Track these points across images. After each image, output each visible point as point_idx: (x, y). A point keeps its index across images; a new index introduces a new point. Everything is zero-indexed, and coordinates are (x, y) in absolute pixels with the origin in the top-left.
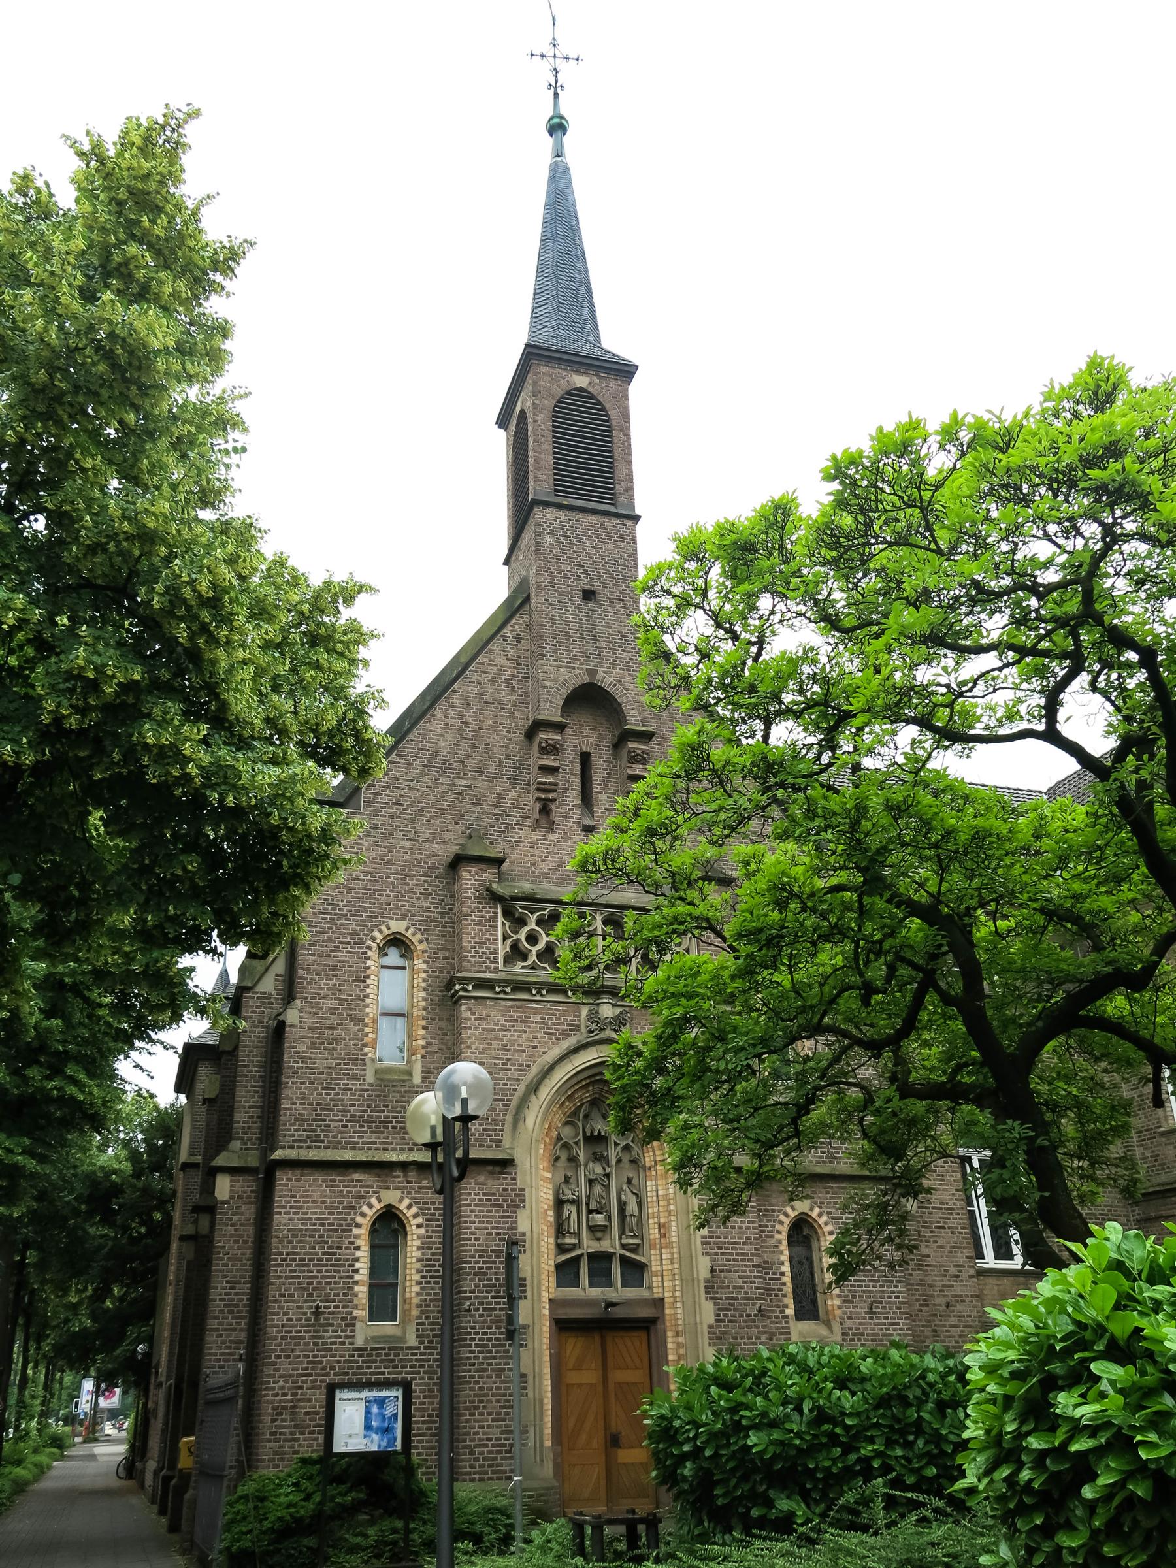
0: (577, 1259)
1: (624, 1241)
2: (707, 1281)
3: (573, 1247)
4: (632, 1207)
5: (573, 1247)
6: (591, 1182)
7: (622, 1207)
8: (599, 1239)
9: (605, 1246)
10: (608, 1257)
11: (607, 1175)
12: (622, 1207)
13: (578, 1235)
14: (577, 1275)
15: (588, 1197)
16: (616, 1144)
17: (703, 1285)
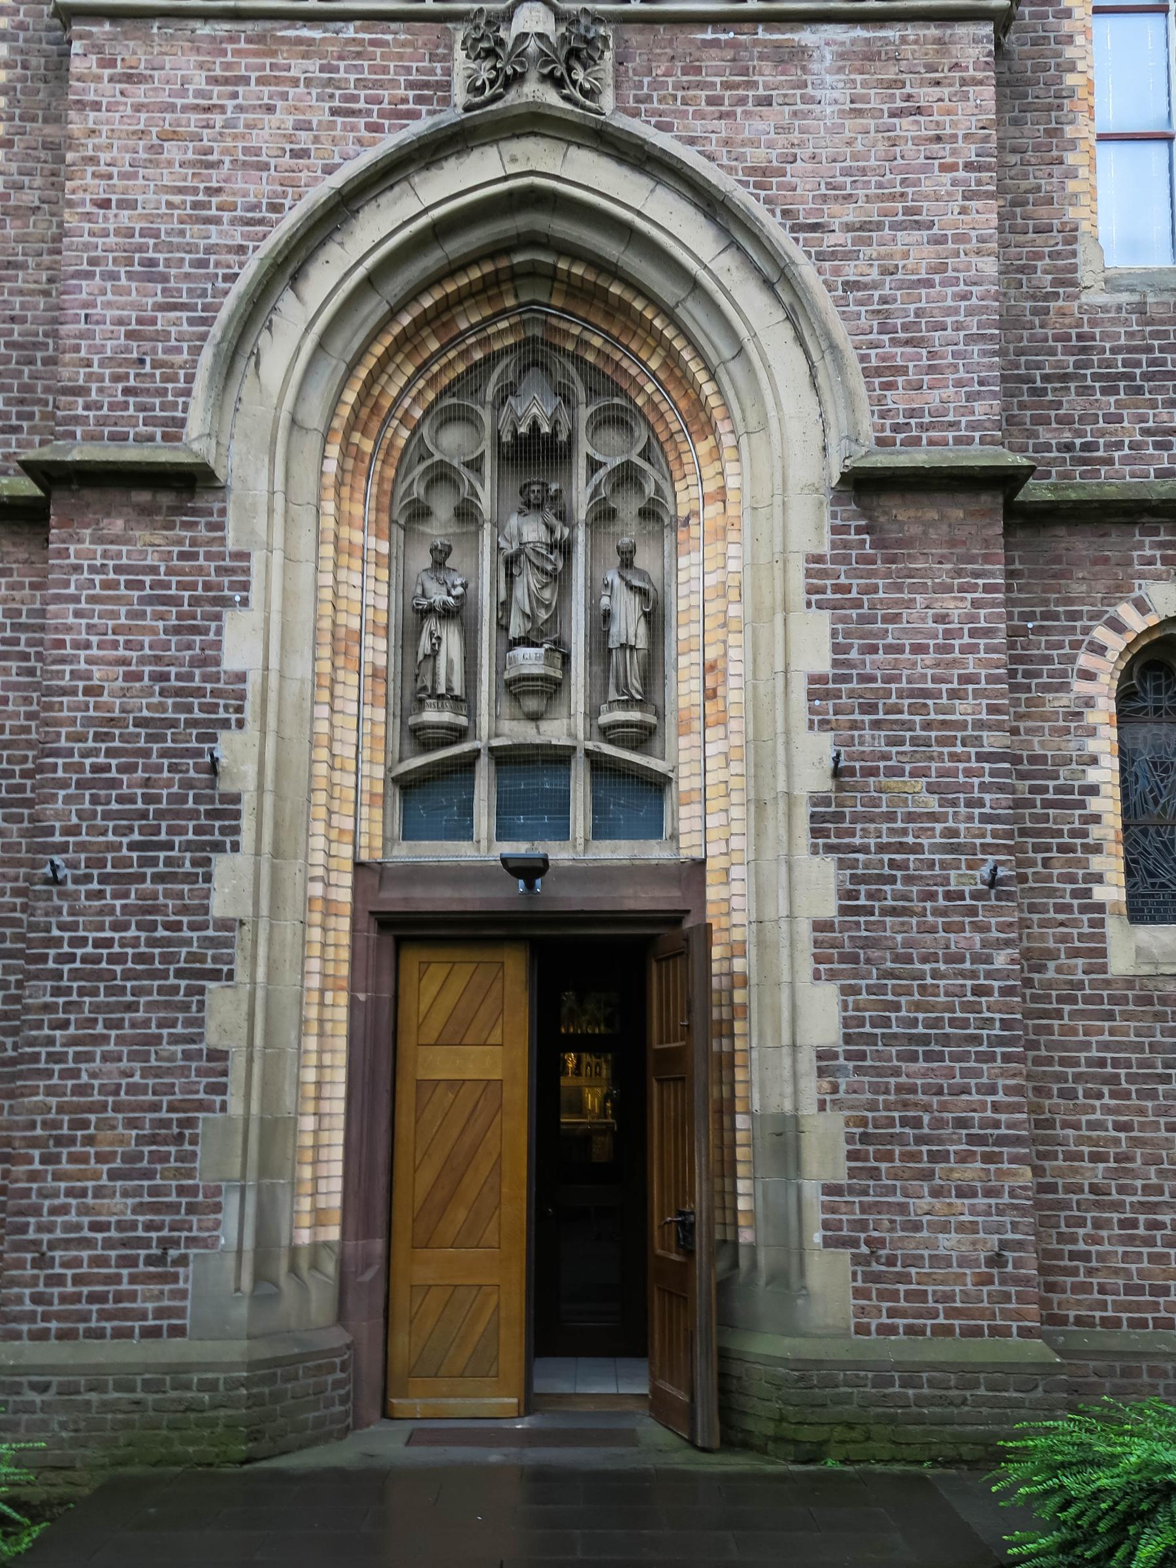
0: (467, 764)
1: (605, 719)
2: (818, 800)
3: (459, 734)
4: (628, 623)
5: (459, 734)
6: (511, 562)
7: (602, 620)
8: (534, 718)
9: (554, 732)
10: (558, 758)
11: (565, 549)
12: (602, 620)
13: (465, 702)
14: (467, 810)
15: (504, 607)
16: (594, 466)
17: (803, 813)
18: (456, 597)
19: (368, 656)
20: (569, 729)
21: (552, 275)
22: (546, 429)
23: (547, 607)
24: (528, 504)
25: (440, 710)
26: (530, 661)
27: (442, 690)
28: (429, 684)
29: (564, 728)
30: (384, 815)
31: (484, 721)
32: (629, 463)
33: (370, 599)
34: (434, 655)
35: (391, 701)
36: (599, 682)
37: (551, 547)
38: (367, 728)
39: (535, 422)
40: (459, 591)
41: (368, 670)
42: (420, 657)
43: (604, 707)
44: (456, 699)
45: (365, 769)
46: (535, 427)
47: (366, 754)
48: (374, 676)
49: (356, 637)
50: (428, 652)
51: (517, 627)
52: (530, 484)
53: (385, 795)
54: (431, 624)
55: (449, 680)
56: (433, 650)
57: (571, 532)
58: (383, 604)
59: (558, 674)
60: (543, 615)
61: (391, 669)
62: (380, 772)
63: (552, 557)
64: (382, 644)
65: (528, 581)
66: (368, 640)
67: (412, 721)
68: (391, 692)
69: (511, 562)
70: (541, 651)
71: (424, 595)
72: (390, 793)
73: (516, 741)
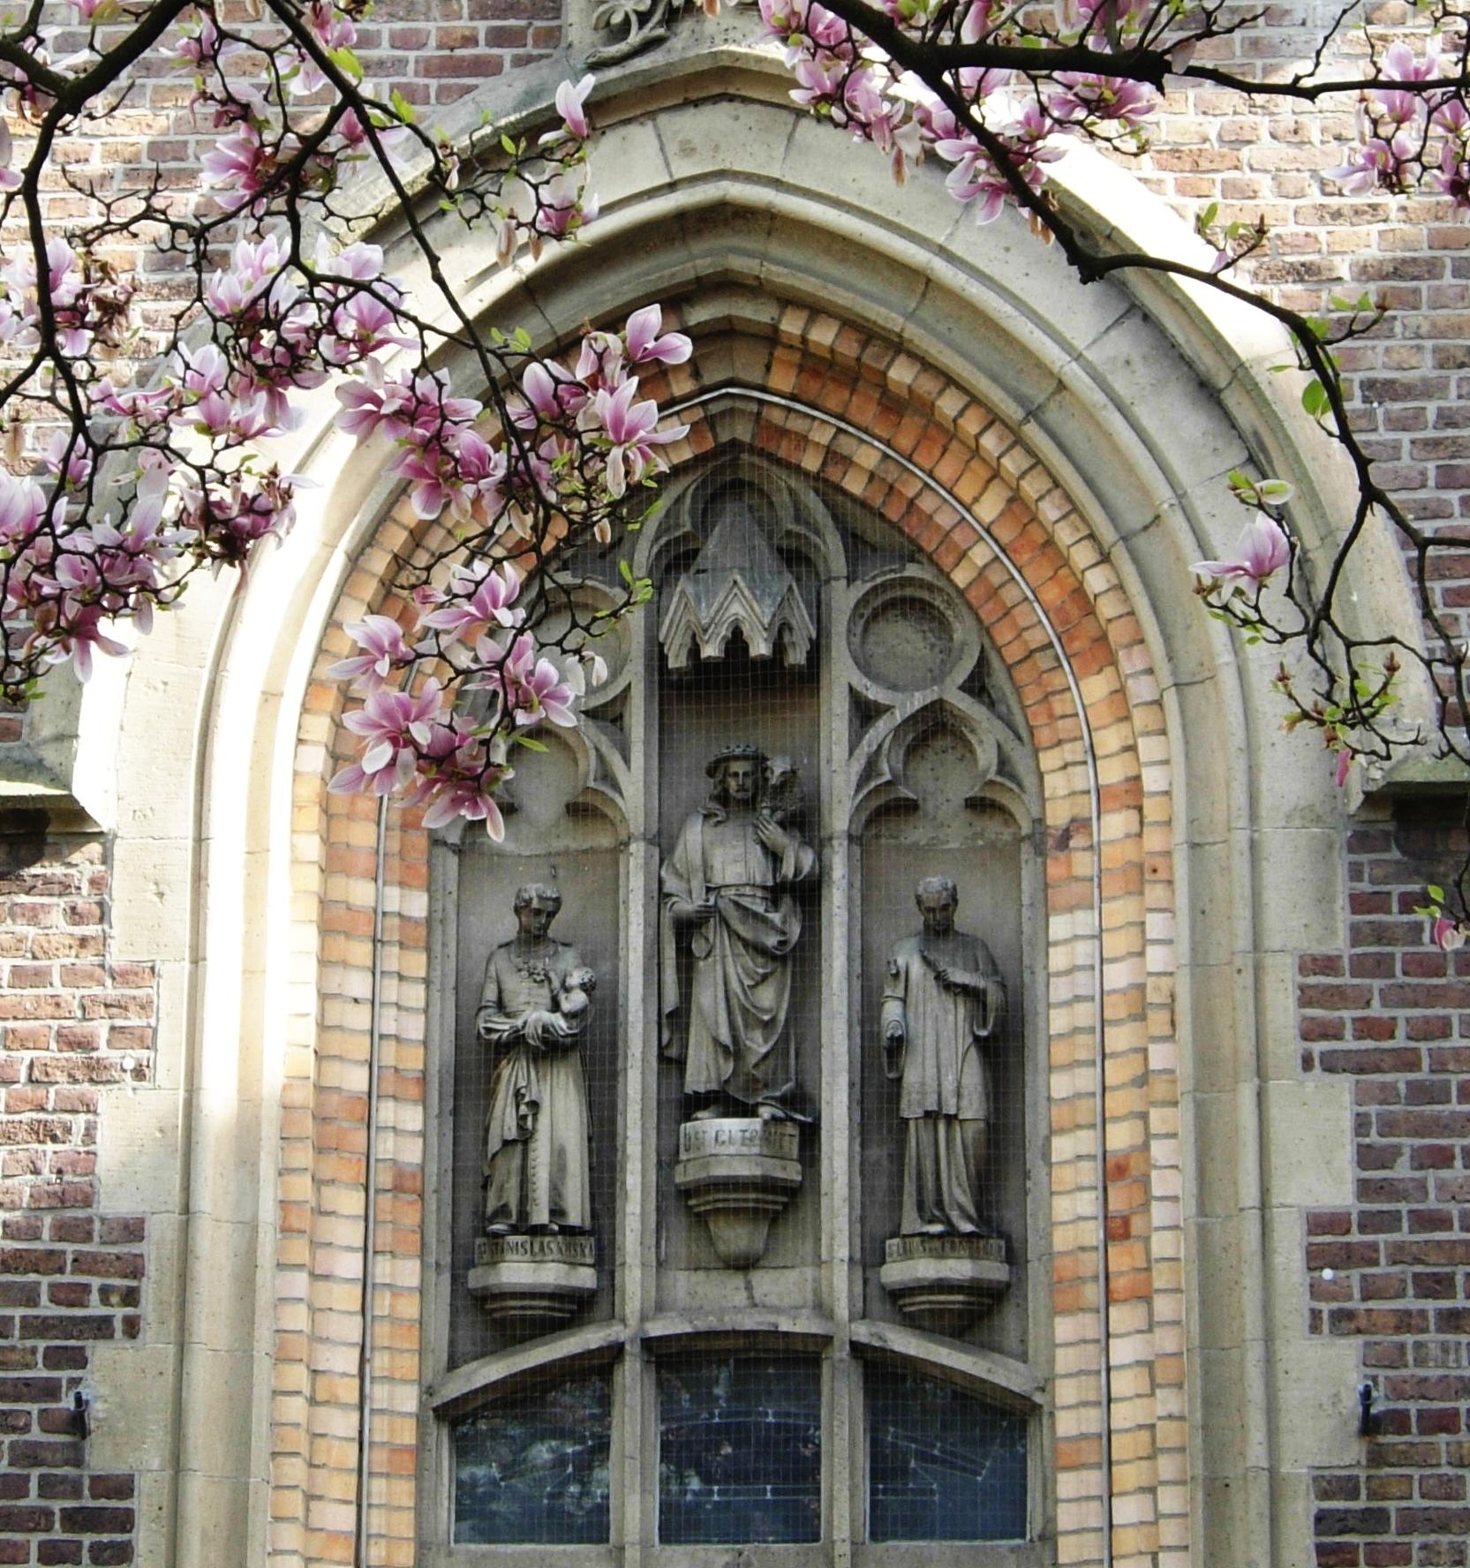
1: (895, 1272)
3: (574, 1308)
9: (779, 1299)
10: (796, 1359)
11: (805, 894)
16: (864, 712)
18: (568, 1016)
19: (386, 1147)
20: (817, 1292)
21: (771, 338)
22: (760, 647)
23: (768, 1026)
24: (723, 798)
25: (537, 1259)
26: (729, 1143)
27: (541, 1216)
28: (513, 1201)
29: (809, 1288)
30: (419, 1494)
31: (634, 1281)
32: (938, 706)
33: (388, 1025)
34: (525, 1138)
35: (432, 1240)
36: (883, 1182)
37: (775, 893)
38: (382, 1304)
39: (737, 632)
40: (577, 1000)
41: (383, 1178)
42: (494, 1145)
43: (893, 1244)
44: (568, 1231)
45: (380, 1395)
46: (736, 642)
47: (380, 1362)
48: (397, 1189)
49: (361, 1110)
50: (512, 1134)
51: (701, 1072)
52: (728, 759)
53: (421, 1446)
54: (514, 1074)
55: (556, 1191)
56: (521, 1128)
57: (819, 856)
58: (414, 1028)
59: (793, 1173)
60: (758, 1045)
61: (433, 1168)
62: (408, 1399)
63: (776, 917)
64: (412, 1118)
65: (723, 973)
66: (386, 1112)
67: (475, 1279)
68: (432, 1228)
69: (687, 929)
70: (754, 1124)
71: (500, 1005)
72: (432, 1441)
73: (702, 1325)
